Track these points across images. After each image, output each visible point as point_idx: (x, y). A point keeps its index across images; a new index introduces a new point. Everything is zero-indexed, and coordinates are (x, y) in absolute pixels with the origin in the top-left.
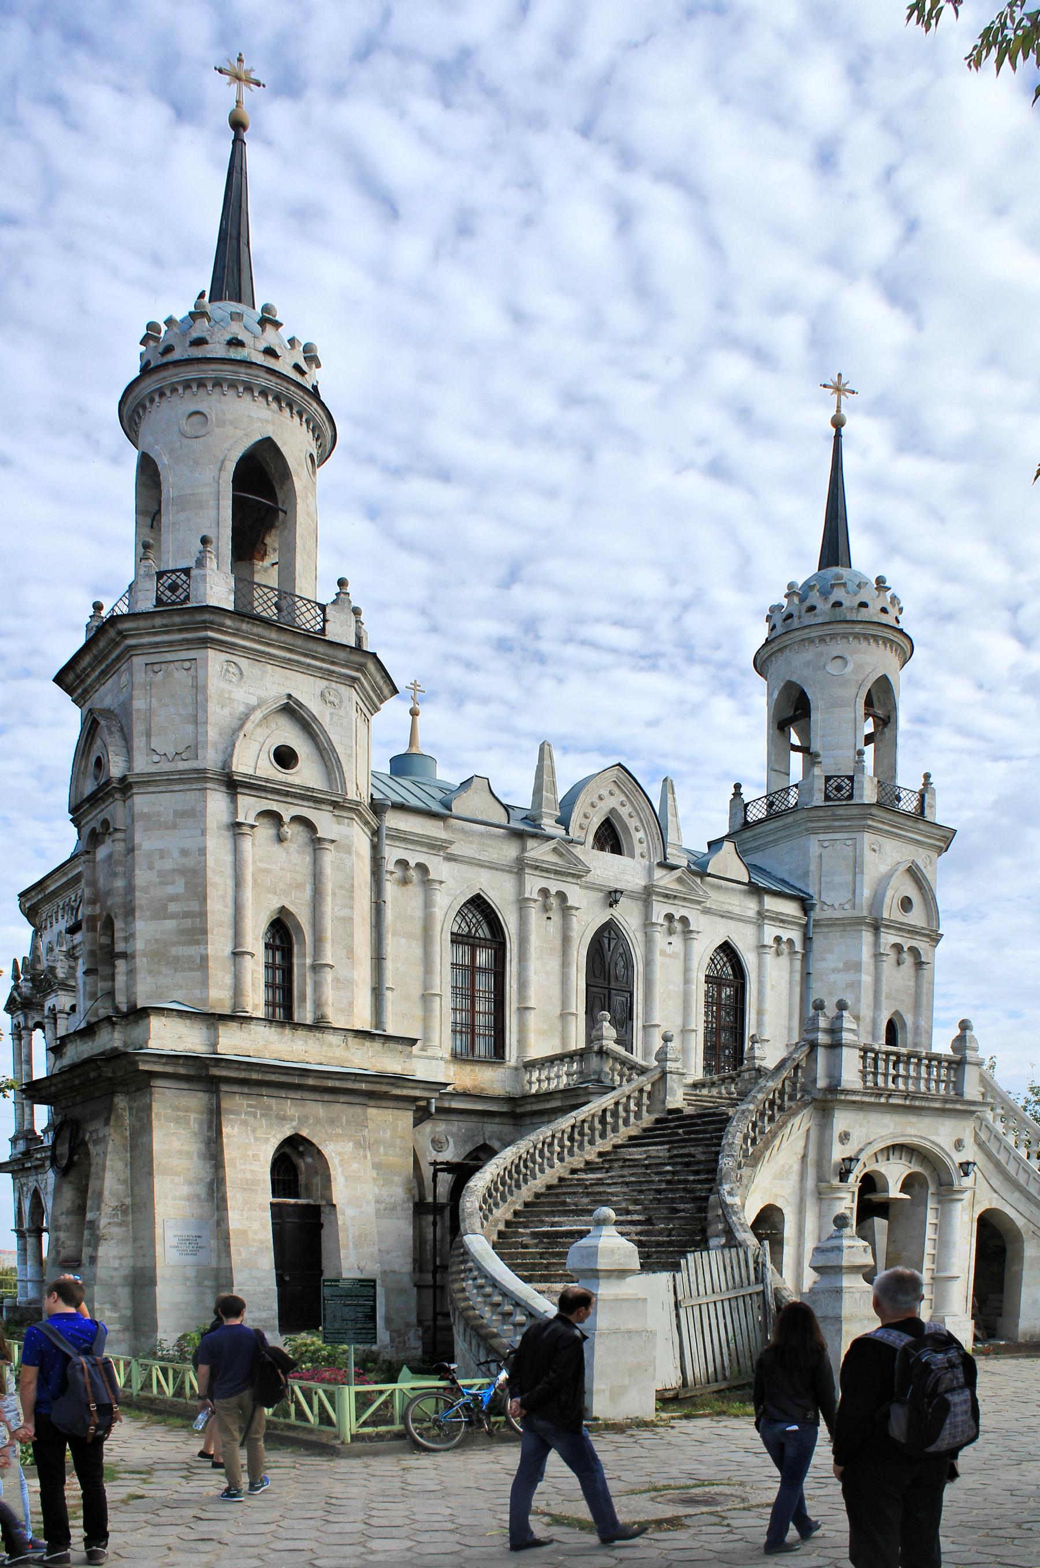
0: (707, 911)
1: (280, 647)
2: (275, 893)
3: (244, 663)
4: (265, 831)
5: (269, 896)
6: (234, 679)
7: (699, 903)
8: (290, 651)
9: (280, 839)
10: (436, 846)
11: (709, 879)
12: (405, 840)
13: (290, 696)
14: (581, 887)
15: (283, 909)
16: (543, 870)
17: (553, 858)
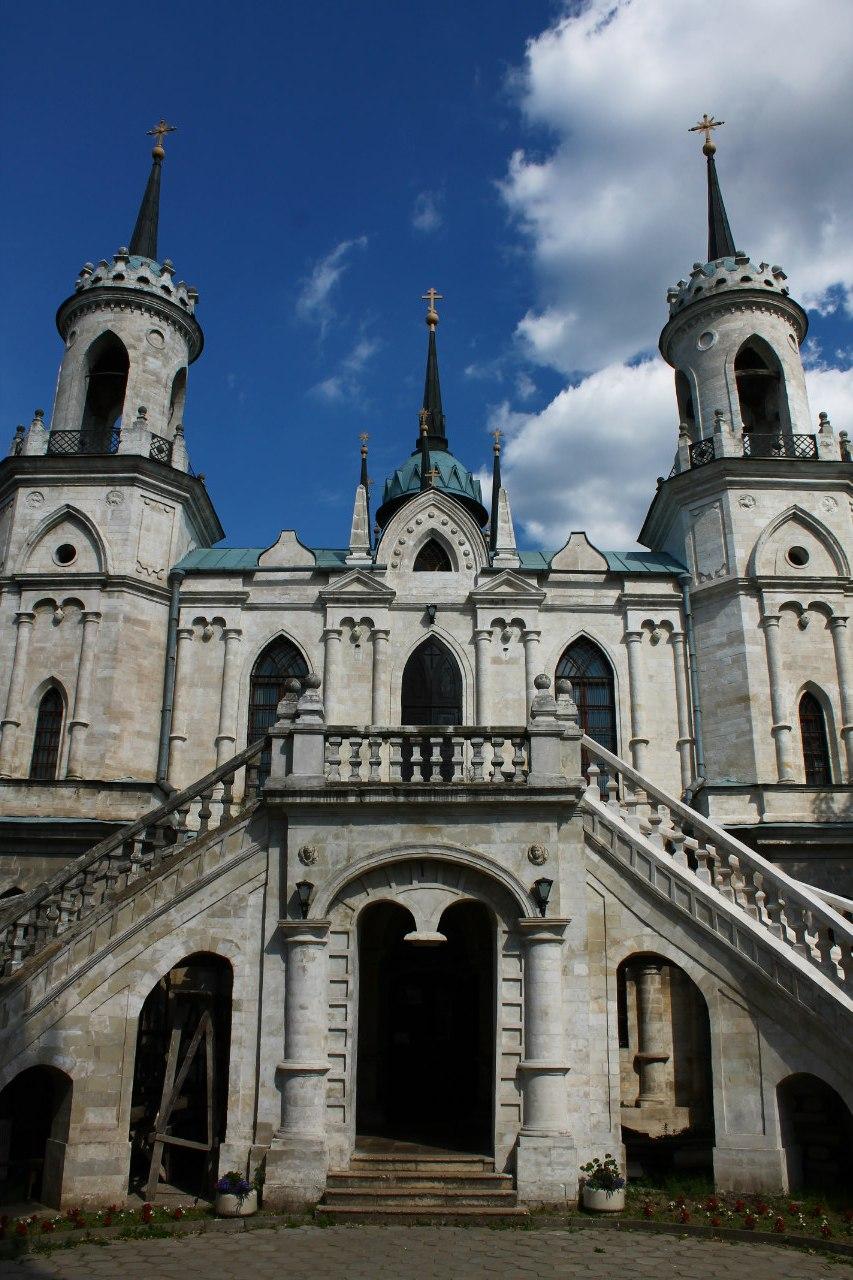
0: (551, 609)
1: (70, 472)
2: (46, 667)
3: (45, 490)
4: (44, 617)
5: (41, 670)
6: (37, 504)
7: (539, 602)
8: (80, 472)
9: (57, 622)
10: (237, 600)
11: (552, 575)
12: (202, 601)
13: (68, 506)
14: (390, 609)
15: (53, 680)
16: (345, 601)
17: (356, 587)
